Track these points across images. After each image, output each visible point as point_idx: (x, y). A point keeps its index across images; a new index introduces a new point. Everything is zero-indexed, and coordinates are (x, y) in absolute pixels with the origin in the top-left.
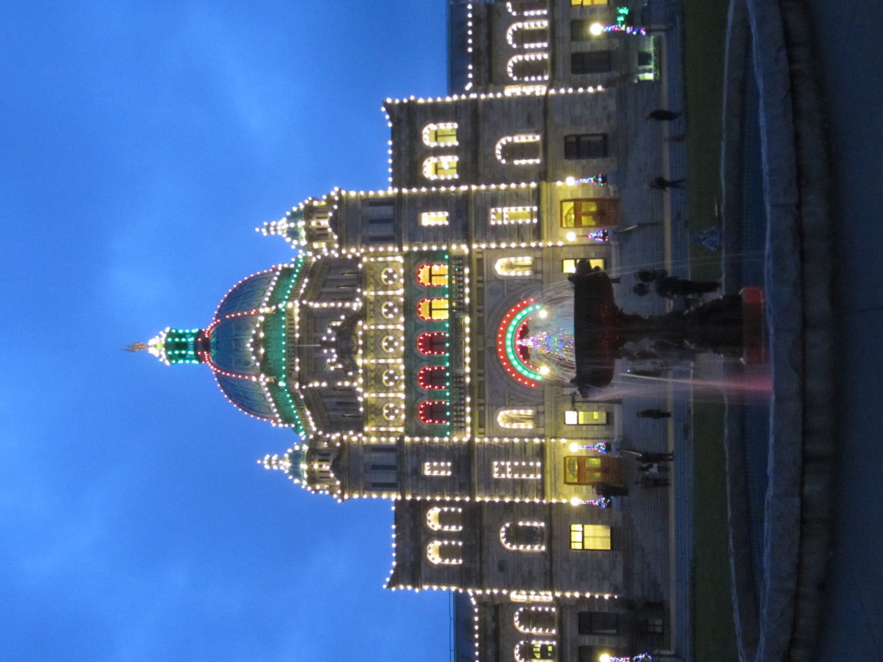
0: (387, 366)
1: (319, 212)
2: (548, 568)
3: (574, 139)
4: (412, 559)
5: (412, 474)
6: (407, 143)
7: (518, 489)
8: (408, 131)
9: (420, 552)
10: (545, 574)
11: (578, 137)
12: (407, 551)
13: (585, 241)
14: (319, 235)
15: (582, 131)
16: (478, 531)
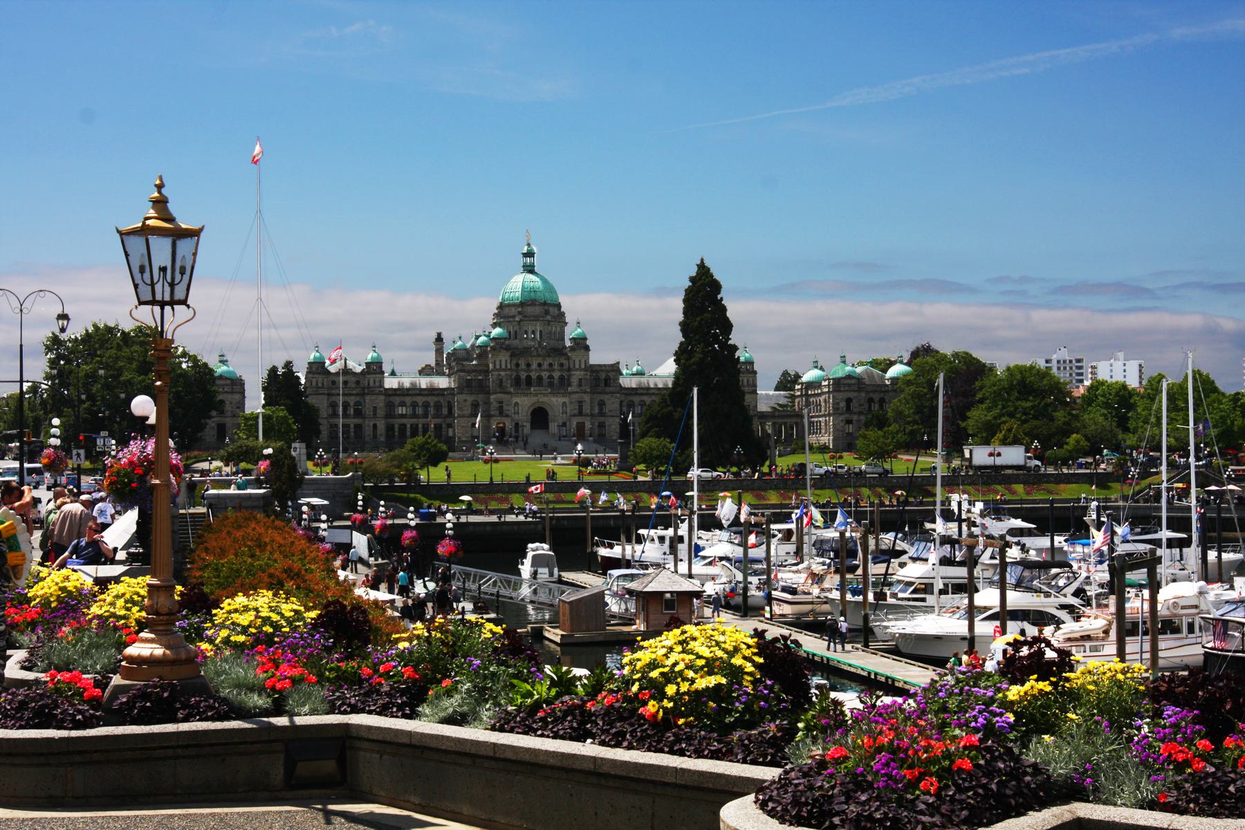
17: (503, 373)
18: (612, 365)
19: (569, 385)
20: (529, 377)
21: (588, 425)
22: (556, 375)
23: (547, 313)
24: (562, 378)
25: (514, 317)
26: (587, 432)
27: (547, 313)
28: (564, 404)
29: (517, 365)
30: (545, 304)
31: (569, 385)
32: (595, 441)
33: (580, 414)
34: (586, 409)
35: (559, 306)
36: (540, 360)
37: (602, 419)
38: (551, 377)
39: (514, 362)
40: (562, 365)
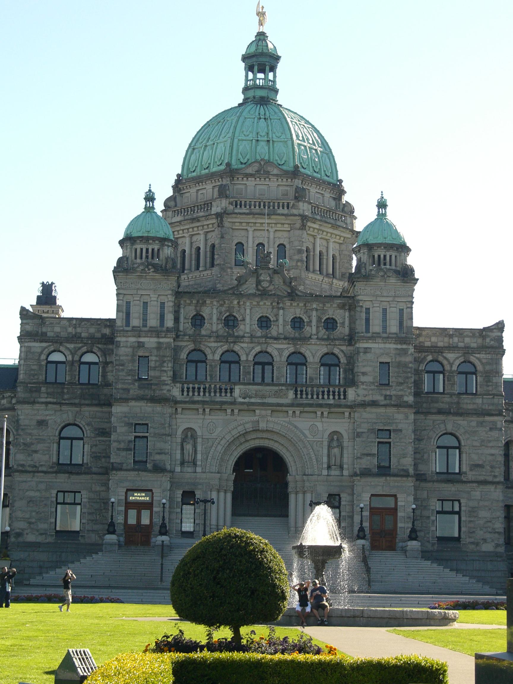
0: (244, 320)
1: (396, 256)
2: (40, 469)
3: (457, 509)
4: (48, 334)
5: (139, 342)
6: (461, 345)
7: (122, 446)
8: (474, 345)
9: (57, 342)
10: (35, 466)
11: (459, 513)
12: (57, 329)
13: (357, 518)
14: (374, 256)
15: (463, 519)
16: (77, 401)
17: (150, 342)
18: (483, 332)
19: (351, 382)
20: (230, 360)
21: (406, 504)
22: (314, 352)
23: (300, 195)
24: (329, 362)
25: (208, 205)
26: (404, 526)
27: (300, 195)
28: (335, 438)
29: (198, 320)
30: (295, 173)
31: (351, 382)
32: (426, 555)
33: (384, 471)
34: (403, 456)
35: (338, 190)
36: (265, 308)
37: (449, 490)
38: (297, 361)
39: (188, 311)
40: (330, 324)
